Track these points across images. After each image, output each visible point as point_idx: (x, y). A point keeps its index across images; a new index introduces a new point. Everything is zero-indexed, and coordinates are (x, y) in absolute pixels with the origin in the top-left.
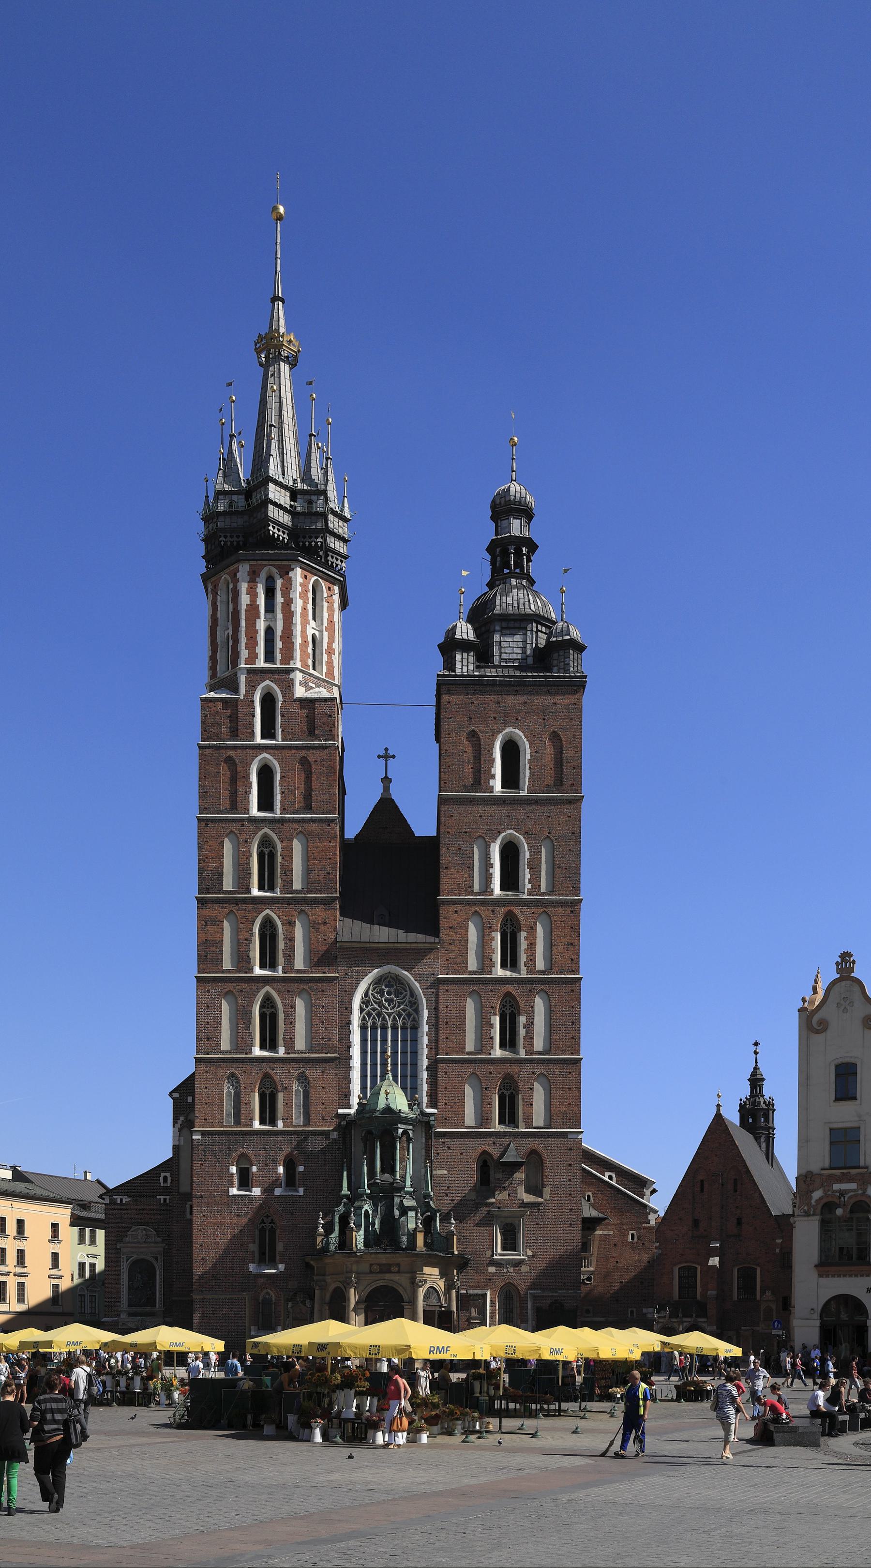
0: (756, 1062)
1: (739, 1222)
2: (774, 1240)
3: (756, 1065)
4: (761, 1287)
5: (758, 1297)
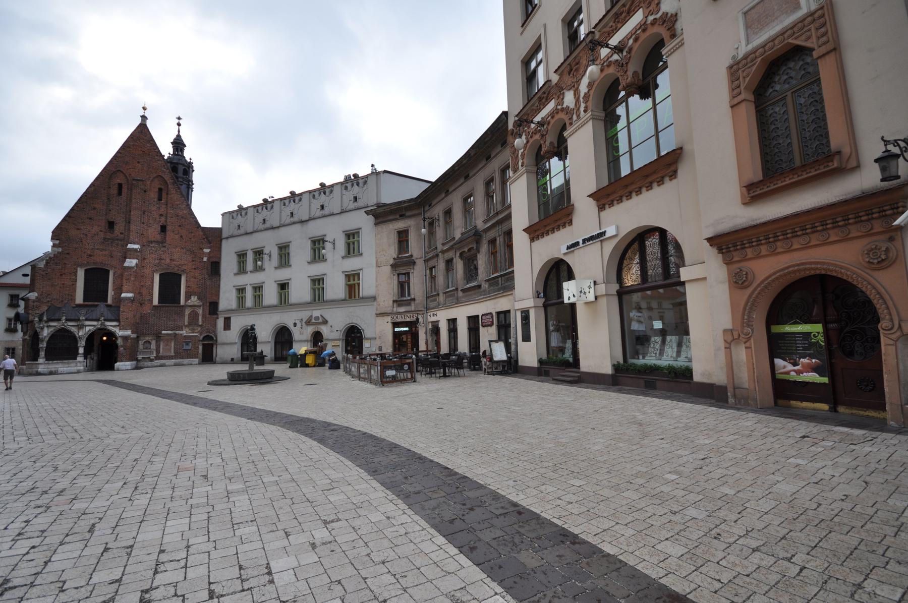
0: (179, 132)
1: (163, 229)
2: (202, 249)
3: (179, 134)
4: (186, 293)
5: (182, 302)
